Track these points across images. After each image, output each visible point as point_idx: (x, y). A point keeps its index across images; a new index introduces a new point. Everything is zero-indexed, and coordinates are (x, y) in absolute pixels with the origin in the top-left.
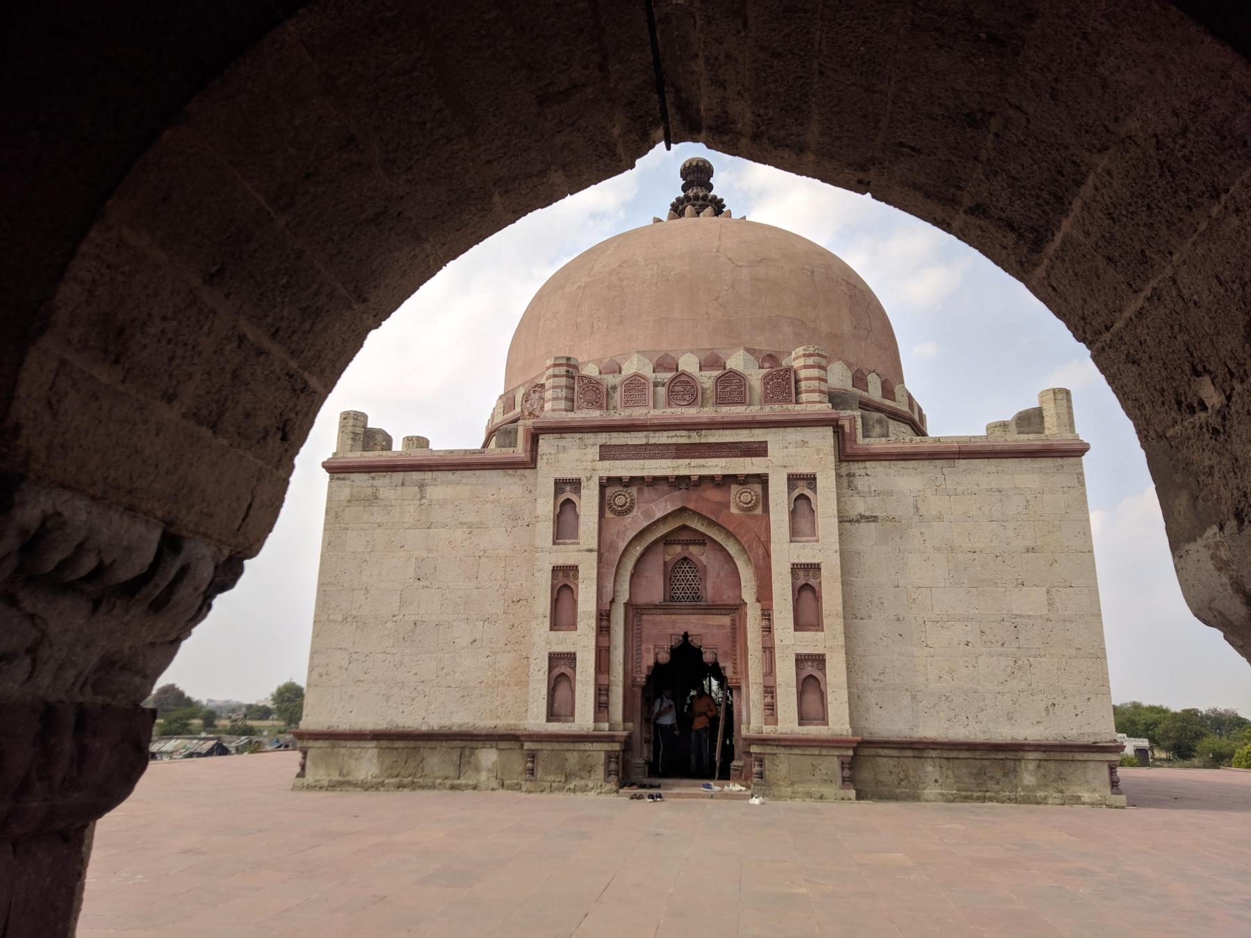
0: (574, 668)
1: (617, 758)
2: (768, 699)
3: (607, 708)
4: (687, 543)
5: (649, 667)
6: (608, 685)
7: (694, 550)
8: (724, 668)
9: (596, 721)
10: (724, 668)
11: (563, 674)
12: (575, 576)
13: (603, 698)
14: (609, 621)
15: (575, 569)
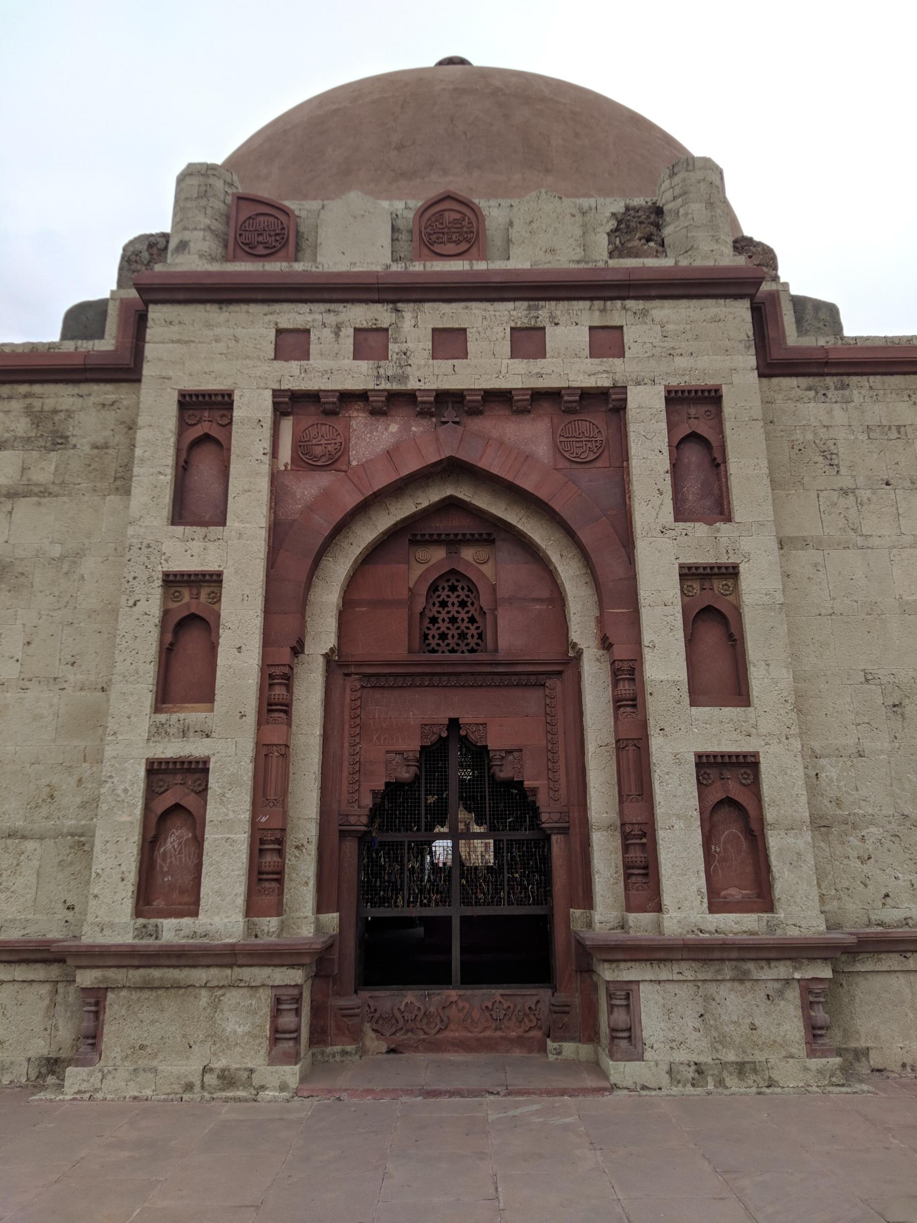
0: (203, 791)
1: (298, 1000)
2: (636, 855)
3: (280, 881)
4: (453, 543)
5: (374, 793)
6: (283, 830)
7: (468, 554)
8: (534, 791)
9: (251, 910)
10: (534, 791)
11: (177, 808)
12: (216, 599)
13: (270, 859)
14: (289, 687)
15: (214, 579)
